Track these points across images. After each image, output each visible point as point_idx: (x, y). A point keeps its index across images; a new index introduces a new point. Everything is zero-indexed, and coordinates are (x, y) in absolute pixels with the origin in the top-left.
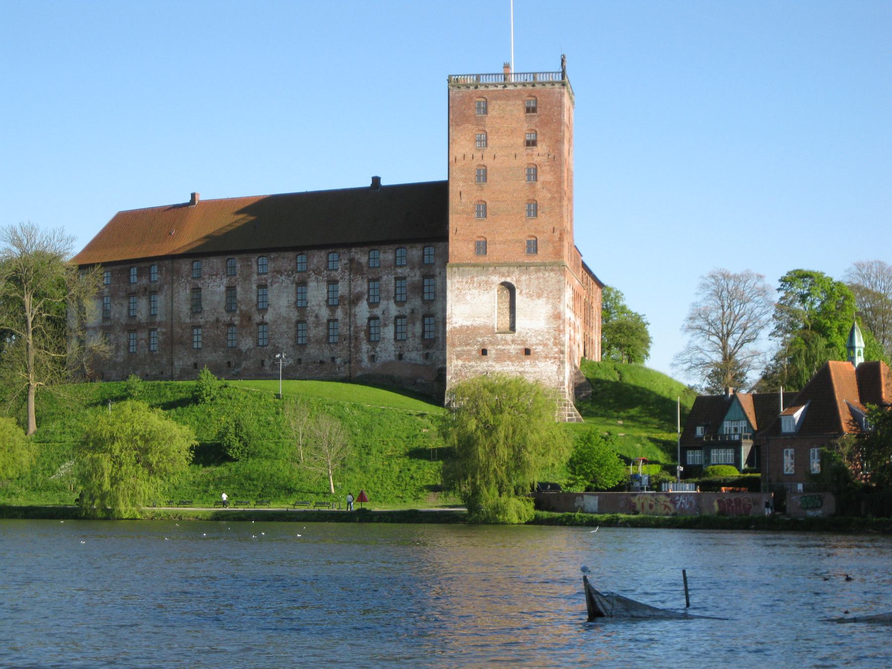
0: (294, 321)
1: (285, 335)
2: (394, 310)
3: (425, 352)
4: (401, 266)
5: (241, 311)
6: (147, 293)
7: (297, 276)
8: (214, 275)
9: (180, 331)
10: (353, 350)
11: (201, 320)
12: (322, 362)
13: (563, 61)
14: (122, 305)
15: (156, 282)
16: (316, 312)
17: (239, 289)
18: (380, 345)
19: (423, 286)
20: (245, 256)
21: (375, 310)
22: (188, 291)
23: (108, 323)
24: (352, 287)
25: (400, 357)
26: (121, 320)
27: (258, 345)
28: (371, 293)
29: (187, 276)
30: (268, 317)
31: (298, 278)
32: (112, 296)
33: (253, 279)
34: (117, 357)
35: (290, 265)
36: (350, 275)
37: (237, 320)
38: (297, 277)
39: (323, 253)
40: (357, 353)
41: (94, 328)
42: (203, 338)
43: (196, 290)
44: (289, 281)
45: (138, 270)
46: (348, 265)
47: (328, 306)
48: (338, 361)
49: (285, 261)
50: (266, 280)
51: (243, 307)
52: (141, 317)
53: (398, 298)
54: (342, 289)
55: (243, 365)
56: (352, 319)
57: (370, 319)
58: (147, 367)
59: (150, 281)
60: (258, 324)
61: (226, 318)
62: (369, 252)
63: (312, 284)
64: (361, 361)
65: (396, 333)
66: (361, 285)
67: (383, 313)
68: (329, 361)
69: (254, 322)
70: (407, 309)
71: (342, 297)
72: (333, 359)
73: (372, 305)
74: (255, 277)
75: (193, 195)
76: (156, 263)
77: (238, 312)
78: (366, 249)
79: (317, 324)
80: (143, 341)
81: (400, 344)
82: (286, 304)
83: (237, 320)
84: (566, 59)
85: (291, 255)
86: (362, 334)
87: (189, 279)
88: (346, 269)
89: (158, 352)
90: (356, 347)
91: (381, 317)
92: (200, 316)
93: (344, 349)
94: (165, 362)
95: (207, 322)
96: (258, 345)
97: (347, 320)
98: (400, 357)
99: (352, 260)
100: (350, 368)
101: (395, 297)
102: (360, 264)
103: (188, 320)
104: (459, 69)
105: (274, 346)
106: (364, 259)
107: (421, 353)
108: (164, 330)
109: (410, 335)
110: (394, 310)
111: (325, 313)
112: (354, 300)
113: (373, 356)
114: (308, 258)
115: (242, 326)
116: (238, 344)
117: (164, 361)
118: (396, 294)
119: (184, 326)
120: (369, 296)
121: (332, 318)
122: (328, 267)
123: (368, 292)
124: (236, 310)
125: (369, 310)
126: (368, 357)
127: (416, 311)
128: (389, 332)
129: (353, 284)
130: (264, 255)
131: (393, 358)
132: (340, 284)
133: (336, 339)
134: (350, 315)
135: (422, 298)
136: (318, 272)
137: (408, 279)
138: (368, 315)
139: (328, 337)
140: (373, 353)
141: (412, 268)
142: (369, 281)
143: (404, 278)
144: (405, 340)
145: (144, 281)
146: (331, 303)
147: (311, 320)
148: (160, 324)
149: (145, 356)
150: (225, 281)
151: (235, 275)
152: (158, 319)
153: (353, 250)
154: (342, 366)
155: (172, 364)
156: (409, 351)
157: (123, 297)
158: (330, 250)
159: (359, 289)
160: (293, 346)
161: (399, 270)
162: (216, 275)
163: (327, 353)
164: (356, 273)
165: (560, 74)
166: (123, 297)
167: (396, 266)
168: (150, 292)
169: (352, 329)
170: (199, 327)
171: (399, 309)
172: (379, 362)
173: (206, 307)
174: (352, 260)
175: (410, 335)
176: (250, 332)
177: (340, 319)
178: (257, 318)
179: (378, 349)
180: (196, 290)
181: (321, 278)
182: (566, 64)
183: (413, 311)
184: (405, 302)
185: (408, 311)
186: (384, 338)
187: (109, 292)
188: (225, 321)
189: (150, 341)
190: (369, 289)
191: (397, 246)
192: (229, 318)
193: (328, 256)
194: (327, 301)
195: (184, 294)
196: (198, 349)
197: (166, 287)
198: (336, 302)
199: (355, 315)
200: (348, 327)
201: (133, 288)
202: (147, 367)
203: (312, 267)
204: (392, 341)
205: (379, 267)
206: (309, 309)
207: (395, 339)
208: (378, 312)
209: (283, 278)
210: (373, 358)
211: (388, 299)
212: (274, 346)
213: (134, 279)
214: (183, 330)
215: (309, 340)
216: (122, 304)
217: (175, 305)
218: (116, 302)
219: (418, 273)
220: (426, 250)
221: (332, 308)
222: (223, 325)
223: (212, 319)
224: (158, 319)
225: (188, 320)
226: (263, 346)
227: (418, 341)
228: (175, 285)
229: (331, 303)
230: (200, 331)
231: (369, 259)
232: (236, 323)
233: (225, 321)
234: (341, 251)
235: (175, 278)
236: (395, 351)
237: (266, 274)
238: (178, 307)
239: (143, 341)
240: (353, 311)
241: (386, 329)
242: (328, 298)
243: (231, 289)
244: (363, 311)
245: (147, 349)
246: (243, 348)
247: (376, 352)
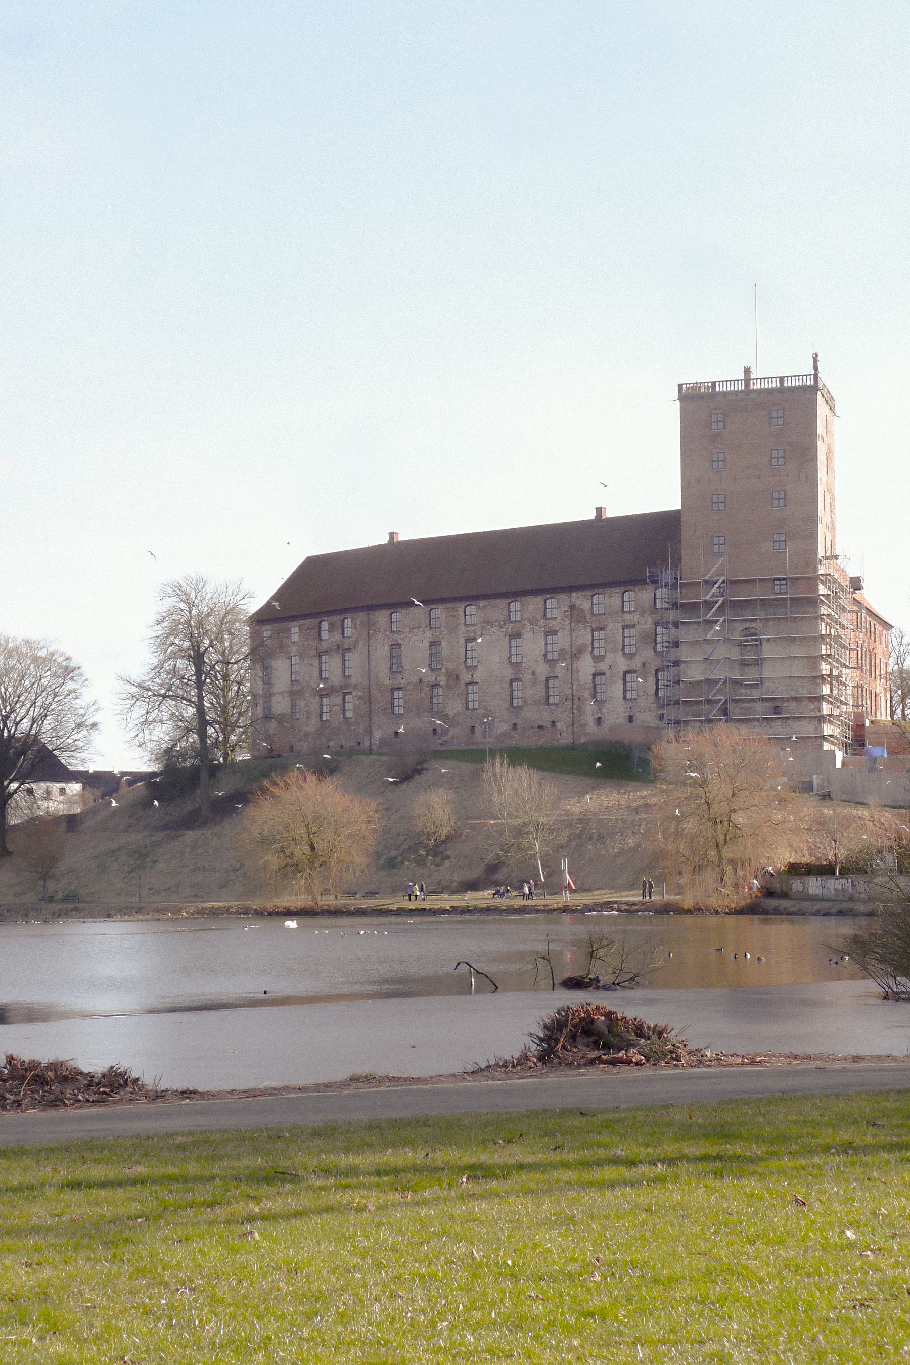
0: (507, 680)
1: (499, 697)
2: (622, 664)
3: (659, 713)
4: (630, 612)
5: (447, 669)
6: (340, 651)
7: (510, 627)
8: (416, 628)
9: (379, 694)
10: (575, 712)
11: (402, 681)
12: (540, 727)
13: (815, 361)
14: (312, 665)
15: (349, 637)
16: (533, 669)
17: (444, 644)
18: (607, 705)
19: (656, 635)
20: (448, 605)
21: (600, 664)
22: (387, 648)
23: (296, 688)
24: (574, 638)
25: (631, 719)
27: (467, 708)
28: (596, 644)
29: (385, 630)
30: (477, 677)
31: (512, 630)
32: (301, 656)
33: (460, 632)
35: (501, 614)
36: (571, 623)
37: (443, 680)
38: (510, 628)
39: (539, 600)
40: (580, 716)
41: (281, 693)
42: (406, 702)
43: (396, 646)
44: (501, 634)
45: (329, 625)
47: (546, 660)
48: (559, 725)
49: (496, 609)
50: (474, 632)
51: (450, 665)
53: (627, 650)
54: (561, 641)
55: (451, 733)
56: (574, 675)
57: (594, 676)
58: (342, 736)
59: (344, 637)
60: (467, 684)
61: (432, 679)
62: (592, 596)
63: (527, 635)
64: (584, 725)
65: (625, 691)
66: (583, 636)
68: (549, 726)
69: (463, 682)
70: (637, 663)
71: (562, 650)
72: (553, 723)
73: (597, 659)
74: (463, 628)
76: (349, 615)
77: (444, 671)
78: (589, 593)
79: (534, 683)
80: (337, 707)
81: (630, 704)
82: (498, 660)
83: (443, 680)
85: (502, 602)
86: (587, 694)
87: (388, 633)
88: (566, 617)
89: (353, 720)
90: (579, 708)
91: (608, 672)
92: (401, 677)
93: (565, 711)
94: (362, 731)
95: (409, 683)
96: (467, 708)
97: (569, 677)
98: (631, 719)
99: (572, 607)
100: (573, 732)
101: (623, 649)
102: (582, 610)
103: (387, 682)
104: (690, 378)
105: (486, 710)
106: (586, 606)
107: (655, 713)
109: (641, 693)
110: (622, 664)
111: (543, 670)
112: (576, 654)
113: (600, 719)
114: (522, 605)
115: (449, 687)
116: (445, 707)
117: (361, 729)
118: (624, 645)
120: (593, 648)
121: (551, 675)
122: (545, 615)
123: (593, 643)
124: (441, 669)
125: (593, 664)
126: (594, 719)
127: (647, 665)
128: (617, 689)
129: (574, 635)
130: (471, 603)
131: (622, 720)
132: (559, 634)
133: (557, 699)
134: (571, 670)
135: (655, 649)
136: (533, 621)
137: (638, 627)
138: (593, 671)
139: (548, 697)
140: (599, 715)
141: (642, 614)
142: (593, 631)
143: (634, 626)
144: (636, 699)
145: (337, 636)
146: (549, 657)
147: (527, 677)
148: (356, 687)
149: (340, 724)
150: (428, 634)
151: (439, 628)
152: (353, 681)
153: (574, 594)
154: (564, 732)
155: (370, 733)
156: (640, 711)
157: (314, 656)
158: (548, 596)
159: (580, 641)
160: (507, 709)
161: (628, 617)
162: (418, 628)
163: (546, 718)
164: (578, 622)
165: (812, 377)
166: (314, 656)
167: (623, 612)
168: (343, 650)
169: (574, 687)
170: (400, 689)
171: (628, 662)
172: (606, 724)
173: (407, 664)
174: (572, 607)
175: (641, 693)
176: (458, 694)
177: (560, 676)
178: (466, 677)
179: (604, 710)
180: (396, 646)
181: (537, 628)
182: (820, 366)
183: (644, 665)
184: (635, 654)
185: (639, 665)
186: (611, 697)
187: (297, 651)
188: (429, 682)
189: (344, 707)
190: (593, 640)
191: (624, 589)
192: (434, 678)
193: (545, 603)
194: (545, 655)
195: (382, 651)
196: (400, 715)
197: (361, 642)
198: (556, 656)
200: (569, 685)
201: (324, 646)
203: (526, 616)
204: (621, 700)
205: (604, 614)
206: (523, 665)
207: (625, 698)
208: (603, 666)
209: (494, 629)
210: (599, 721)
211: (614, 651)
212: (486, 710)
213: (325, 635)
215: (525, 702)
217: (371, 663)
218: (306, 662)
219: (650, 621)
220: (626, 595)
221: (551, 663)
222: (427, 686)
223: (415, 679)
224: (353, 681)
225: (387, 682)
226: (473, 710)
227: (652, 699)
228: (372, 641)
229: (549, 657)
230: (401, 694)
231: (592, 604)
232: (442, 683)
233: (429, 682)
234: (561, 596)
235: (371, 632)
237: (475, 625)
239: (337, 707)
240: (575, 666)
241: (614, 686)
242: (546, 652)
243: (434, 643)
244: (586, 665)
245: (342, 717)
246: (450, 713)
247: (603, 714)
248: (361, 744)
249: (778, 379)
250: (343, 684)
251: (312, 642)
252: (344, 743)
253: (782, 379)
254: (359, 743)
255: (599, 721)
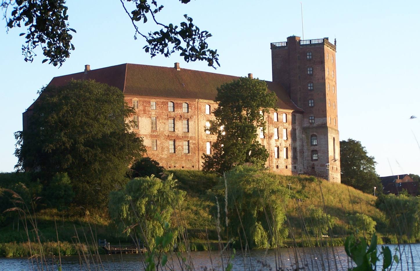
9: (202, 143)
21: (277, 143)
26: (165, 133)
34: (162, 154)
36: (268, 123)
46: (267, 119)
52: (178, 133)
58: (183, 162)
67: (280, 145)
75: (176, 64)
80: (180, 147)
84: (336, 40)
90: (271, 160)
97: (268, 146)
108: (194, 142)
119: (204, 141)
129: (270, 128)
140: (277, 164)
157: (165, 119)
166: (165, 119)
171: (285, 143)
179: (279, 162)
199: (271, 144)
202: (183, 162)
210: (277, 167)
214: (203, 143)
216: (165, 123)
218: (161, 121)
236: (285, 164)
238: (201, 130)
247: (278, 164)
248: (194, 167)
249: (309, 41)
250: (183, 135)
251: (164, 111)
252: (184, 165)
253: (310, 41)
254: (193, 167)
255: (277, 167)
